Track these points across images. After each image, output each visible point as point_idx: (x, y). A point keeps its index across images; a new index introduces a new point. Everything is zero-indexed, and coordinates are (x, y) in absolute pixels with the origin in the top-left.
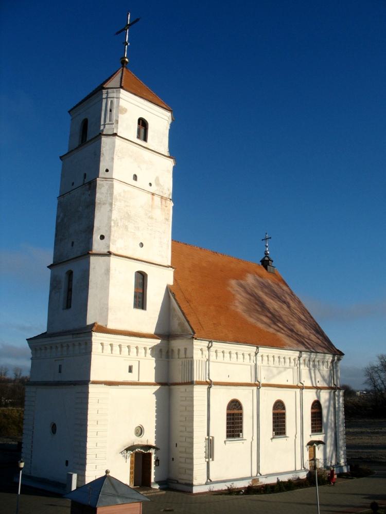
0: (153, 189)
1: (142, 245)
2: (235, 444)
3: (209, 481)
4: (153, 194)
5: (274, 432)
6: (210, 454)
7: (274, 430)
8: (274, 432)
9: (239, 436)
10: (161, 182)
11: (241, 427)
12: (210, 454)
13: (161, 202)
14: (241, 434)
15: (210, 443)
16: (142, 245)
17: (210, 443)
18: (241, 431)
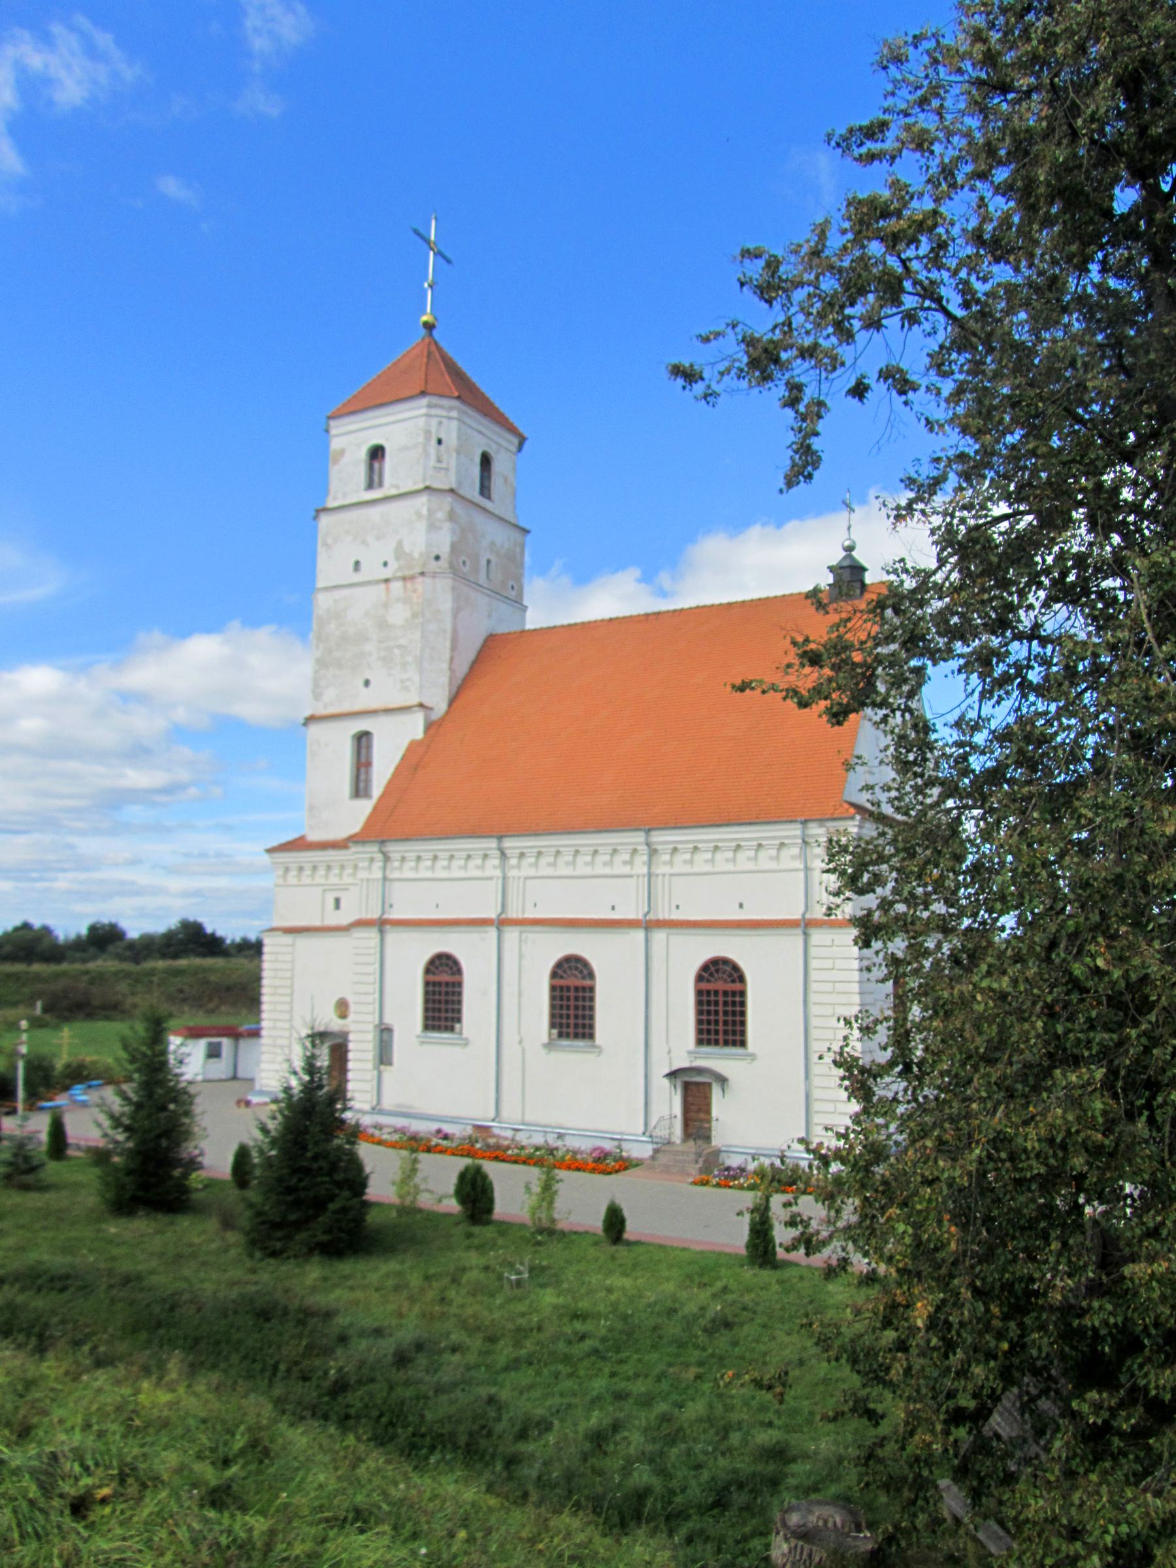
0: (387, 573)
1: (367, 683)
2: (441, 1047)
3: (376, 1110)
4: (387, 581)
5: (555, 1031)
6: (384, 1056)
7: (553, 1025)
8: (555, 1031)
9: (452, 1029)
10: (407, 548)
11: (459, 1011)
12: (384, 1056)
13: (405, 588)
14: (457, 1026)
15: (385, 1033)
16: (367, 683)
17: (385, 1033)
18: (459, 1020)
